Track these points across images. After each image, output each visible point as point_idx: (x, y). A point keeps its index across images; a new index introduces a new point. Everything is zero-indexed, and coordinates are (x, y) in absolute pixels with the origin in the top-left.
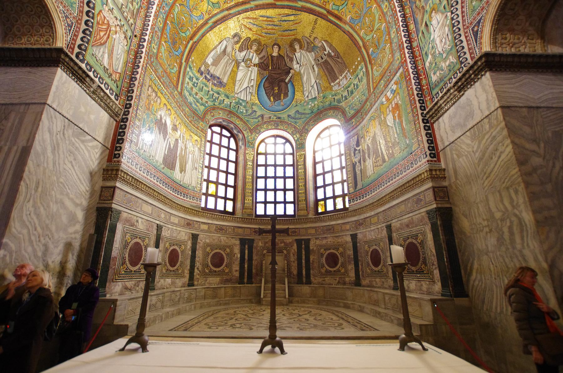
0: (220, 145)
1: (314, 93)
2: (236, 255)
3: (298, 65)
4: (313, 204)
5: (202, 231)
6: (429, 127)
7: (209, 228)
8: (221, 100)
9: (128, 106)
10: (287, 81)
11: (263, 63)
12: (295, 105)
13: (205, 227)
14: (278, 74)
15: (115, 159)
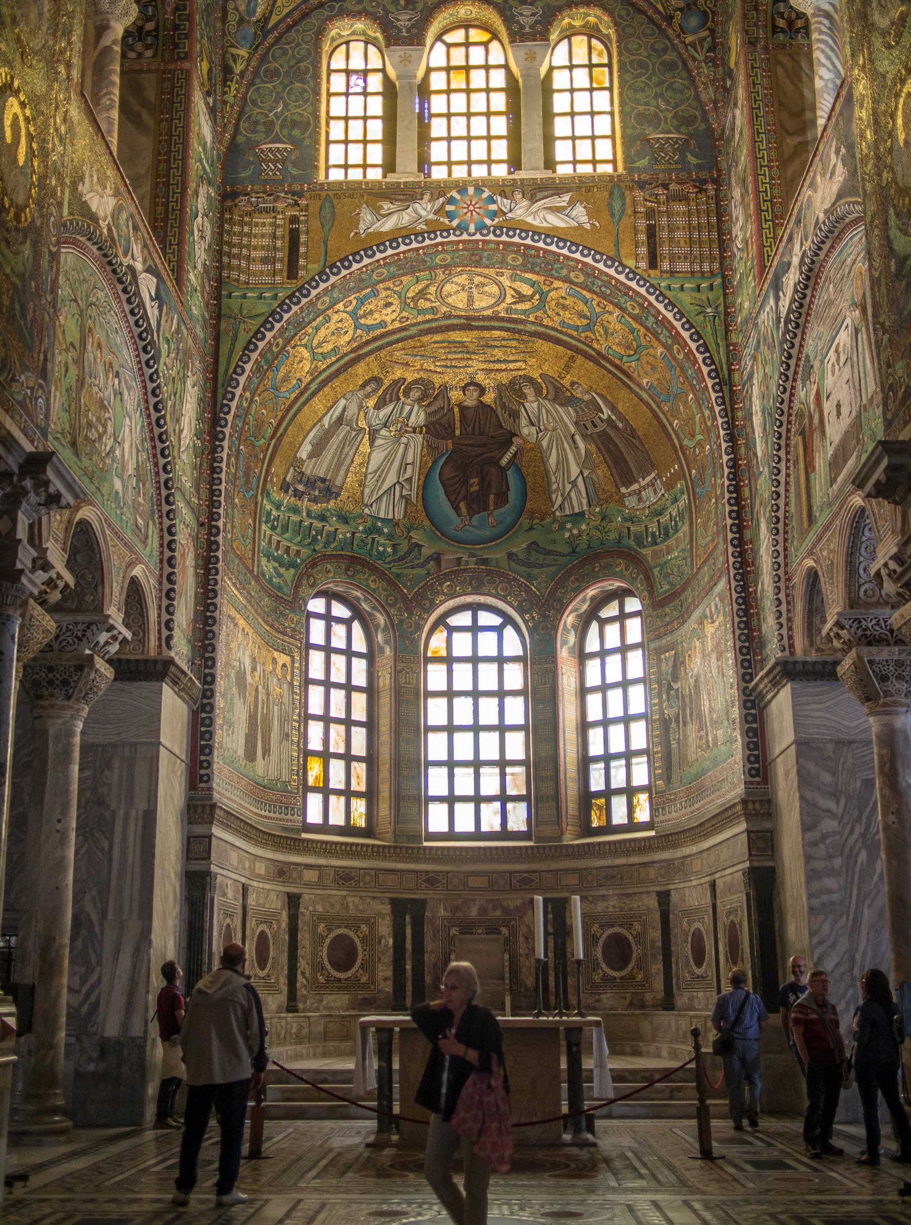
0: (328, 650)
1: (579, 502)
2: (383, 941)
3: (533, 430)
4: (576, 806)
5: (308, 885)
6: (754, 716)
7: (320, 877)
8: (328, 535)
9: (209, 680)
10: (504, 461)
11: (436, 422)
12: (528, 526)
13: (311, 876)
14: (478, 446)
15: (203, 785)
